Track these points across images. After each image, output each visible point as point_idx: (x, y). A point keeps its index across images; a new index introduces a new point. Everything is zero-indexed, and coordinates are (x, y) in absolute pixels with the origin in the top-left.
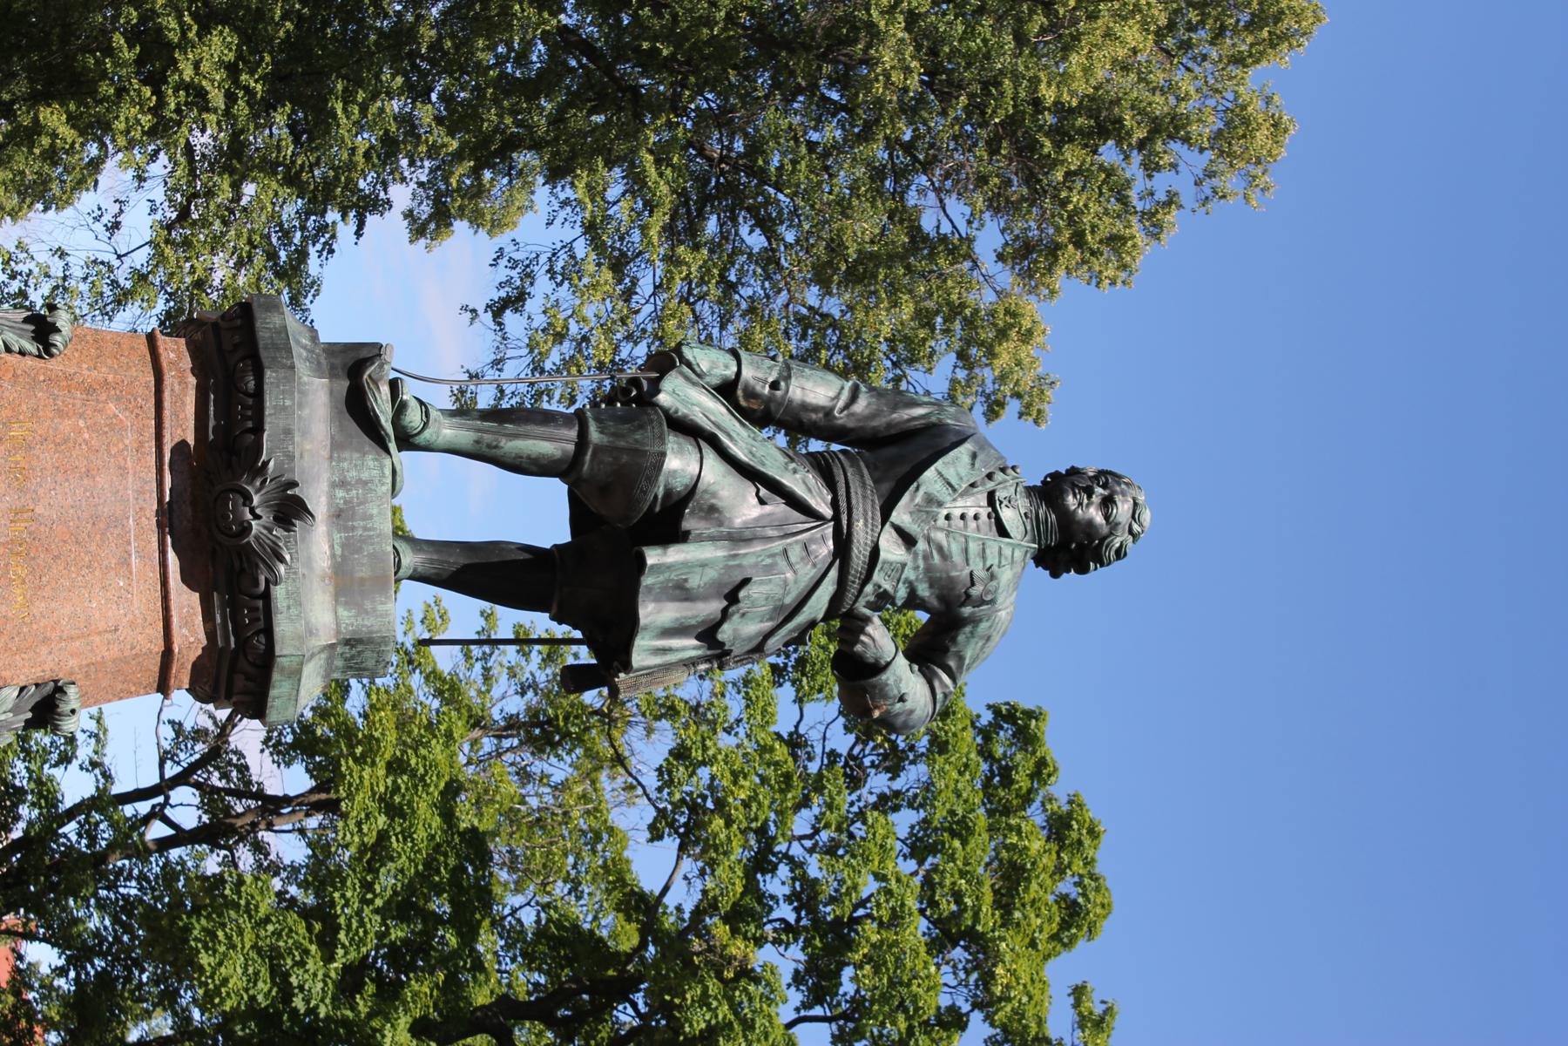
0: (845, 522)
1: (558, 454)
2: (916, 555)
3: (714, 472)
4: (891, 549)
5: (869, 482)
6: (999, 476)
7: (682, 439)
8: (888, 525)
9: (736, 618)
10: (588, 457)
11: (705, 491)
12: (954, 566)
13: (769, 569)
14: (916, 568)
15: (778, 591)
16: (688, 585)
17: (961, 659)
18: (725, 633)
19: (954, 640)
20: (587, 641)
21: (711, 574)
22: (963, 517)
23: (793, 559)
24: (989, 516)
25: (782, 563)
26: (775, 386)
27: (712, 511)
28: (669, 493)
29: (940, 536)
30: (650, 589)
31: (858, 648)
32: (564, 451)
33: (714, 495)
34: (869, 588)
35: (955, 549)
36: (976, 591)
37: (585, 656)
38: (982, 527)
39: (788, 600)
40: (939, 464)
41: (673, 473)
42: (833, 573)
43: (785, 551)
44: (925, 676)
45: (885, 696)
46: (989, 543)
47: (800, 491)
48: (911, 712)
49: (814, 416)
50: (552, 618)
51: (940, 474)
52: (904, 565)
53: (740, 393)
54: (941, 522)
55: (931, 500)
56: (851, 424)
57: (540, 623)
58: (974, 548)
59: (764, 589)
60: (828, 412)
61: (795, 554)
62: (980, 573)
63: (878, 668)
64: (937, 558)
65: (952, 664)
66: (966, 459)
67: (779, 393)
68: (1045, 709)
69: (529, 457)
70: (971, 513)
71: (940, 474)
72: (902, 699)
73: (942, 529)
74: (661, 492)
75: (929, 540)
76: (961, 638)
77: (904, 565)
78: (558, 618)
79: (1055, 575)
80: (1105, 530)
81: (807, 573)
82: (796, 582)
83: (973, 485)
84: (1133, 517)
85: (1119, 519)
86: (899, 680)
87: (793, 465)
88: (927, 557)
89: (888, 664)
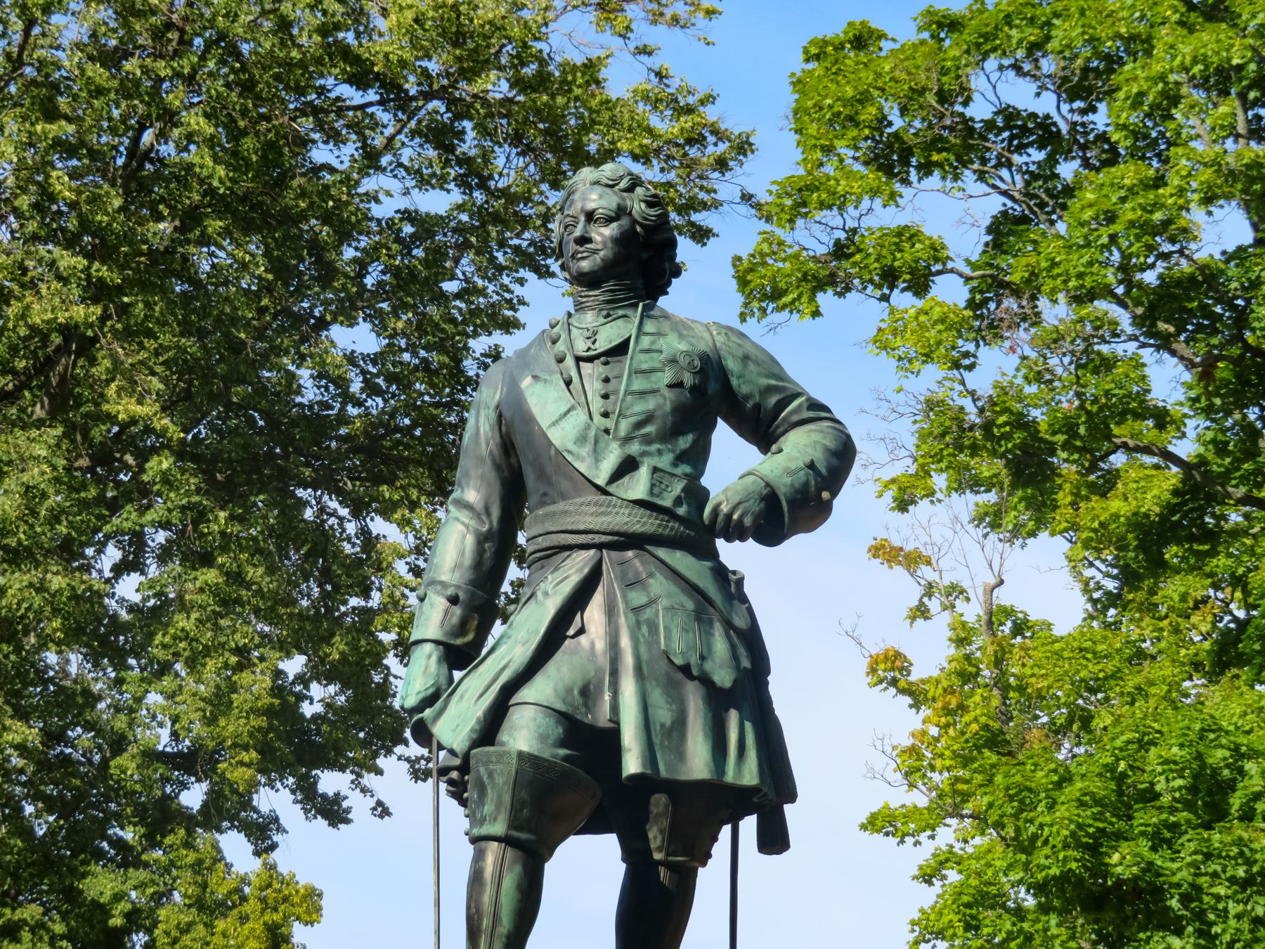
0: (604, 538)
1: (518, 868)
2: (644, 454)
3: (541, 689)
4: (638, 485)
5: (561, 506)
6: (561, 347)
7: (506, 725)
8: (611, 489)
9: (708, 666)
10: (523, 836)
11: (564, 701)
12: (659, 407)
13: (653, 627)
14: (660, 452)
15: (679, 619)
16: (668, 723)
17: (769, 390)
18: (723, 677)
19: (747, 397)
20: (735, 821)
21: (656, 696)
22: (605, 397)
23: (644, 600)
24: (606, 363)
25: (647, 614)
26: (454, 600)
27: (588, 693)
28: (562, 743)
29: (624, 426)
30: (669, 768)
31: (748, 521)
32: (513, 862)
33: (569, 690)
34: (681, 511)
35: (640, 407)
36: (688, 379)
37: (749, 825)
38: (615, 373)
39: (690, 605)
40: (544, 421)
41: (542, 738)
42: (662, 553)
43: (637, 610)
44: (786, 431)
45: (806, 485)
46: (635, 365)
47: (567, 588)
48: (827, 450)
49: (488, 555)
50: (704, 864)
51: (554, 423)
52: (655, 470)
53: (459, 641)
54: (609, 423)
55: (582, 439)
56: (496, 512)
57: (710, 881)
58: (638, 385)
59: (676, 634)
60: (482, 540)
61: (638, 598)
62: (667, 377)
63: (770, 498)
64: (649, 429)
65: (773, 400)
66: (539, 387)
67: (462, 596)
68: (922, 7)
69: (520, 901)
70: (598, 385)
71: (554, 423)
72: (811, 466)
73: (617, 423)
74: (563, 752)
75: (627, 440)
76: (745, 389)
77: (655, 470)
78: (705, 857)
79: (677, 271)
80: (625, 221)
81: (659, 585)
82: (669, 596)
83: (568, 383)
84: (612, 186)
85: (614, 206)
86: (790, 473)
87: (539, 594)
88: (647, 440)
89: (768, 485)
